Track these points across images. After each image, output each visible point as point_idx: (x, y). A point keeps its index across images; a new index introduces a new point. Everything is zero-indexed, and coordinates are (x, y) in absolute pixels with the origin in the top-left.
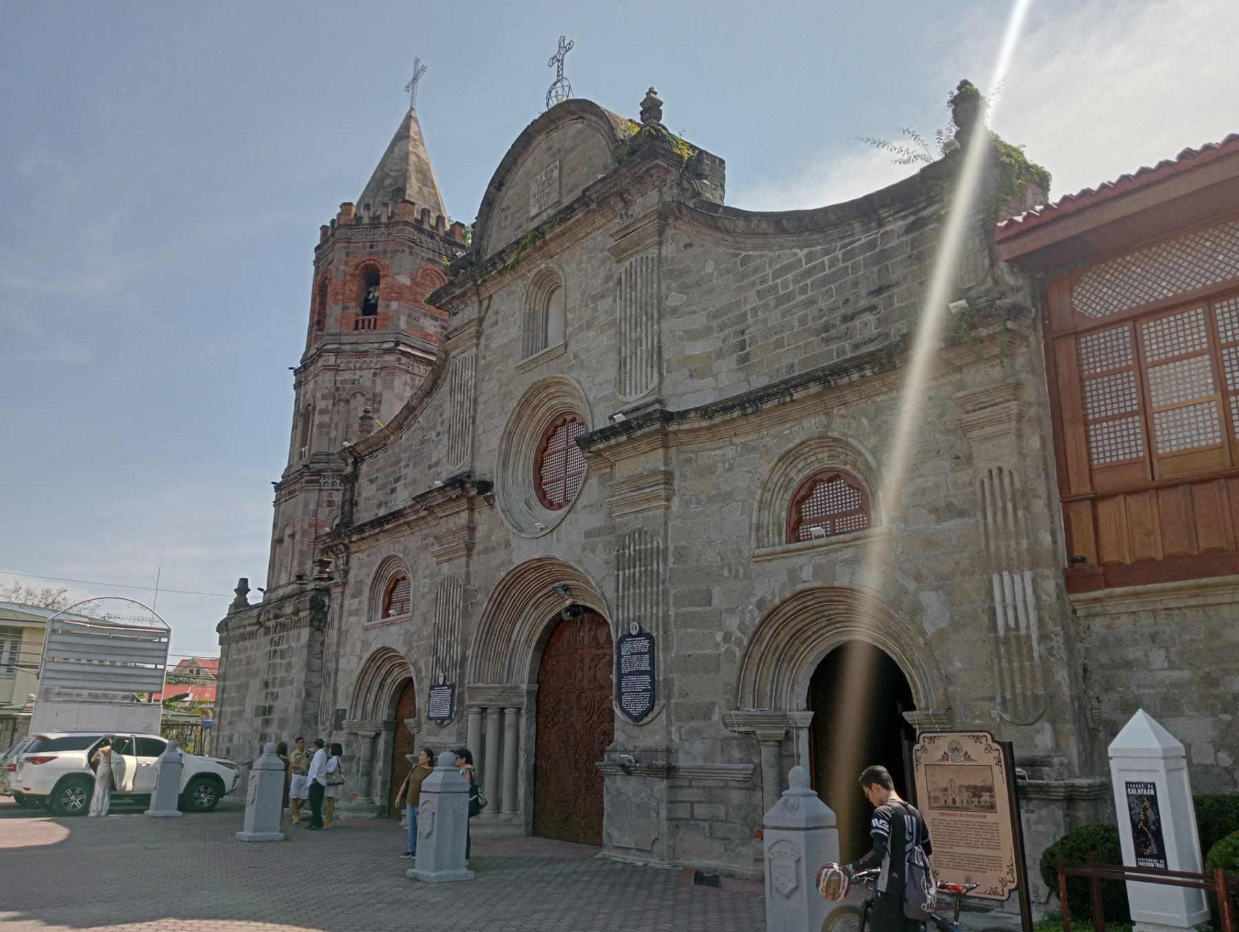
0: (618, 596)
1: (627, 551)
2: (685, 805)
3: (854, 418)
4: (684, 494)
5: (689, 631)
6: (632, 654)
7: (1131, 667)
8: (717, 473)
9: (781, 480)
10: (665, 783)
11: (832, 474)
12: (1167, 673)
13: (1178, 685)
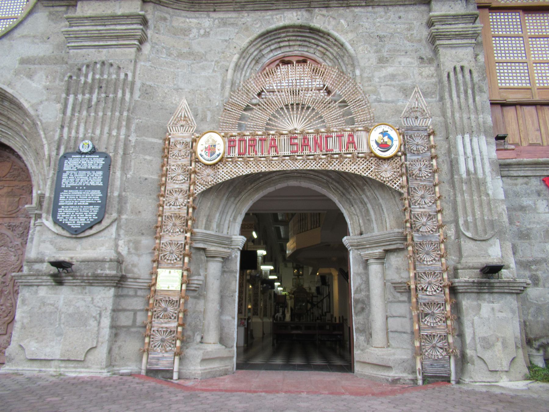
0: (63, 120)
1: (83, 79)
3: (334, 18)
4: (156, 44)
5: (148, 158)
6: (78, 170)
7: (525, 210)
8: (191, 36)
10: (112, 291)
11: (301, 59)
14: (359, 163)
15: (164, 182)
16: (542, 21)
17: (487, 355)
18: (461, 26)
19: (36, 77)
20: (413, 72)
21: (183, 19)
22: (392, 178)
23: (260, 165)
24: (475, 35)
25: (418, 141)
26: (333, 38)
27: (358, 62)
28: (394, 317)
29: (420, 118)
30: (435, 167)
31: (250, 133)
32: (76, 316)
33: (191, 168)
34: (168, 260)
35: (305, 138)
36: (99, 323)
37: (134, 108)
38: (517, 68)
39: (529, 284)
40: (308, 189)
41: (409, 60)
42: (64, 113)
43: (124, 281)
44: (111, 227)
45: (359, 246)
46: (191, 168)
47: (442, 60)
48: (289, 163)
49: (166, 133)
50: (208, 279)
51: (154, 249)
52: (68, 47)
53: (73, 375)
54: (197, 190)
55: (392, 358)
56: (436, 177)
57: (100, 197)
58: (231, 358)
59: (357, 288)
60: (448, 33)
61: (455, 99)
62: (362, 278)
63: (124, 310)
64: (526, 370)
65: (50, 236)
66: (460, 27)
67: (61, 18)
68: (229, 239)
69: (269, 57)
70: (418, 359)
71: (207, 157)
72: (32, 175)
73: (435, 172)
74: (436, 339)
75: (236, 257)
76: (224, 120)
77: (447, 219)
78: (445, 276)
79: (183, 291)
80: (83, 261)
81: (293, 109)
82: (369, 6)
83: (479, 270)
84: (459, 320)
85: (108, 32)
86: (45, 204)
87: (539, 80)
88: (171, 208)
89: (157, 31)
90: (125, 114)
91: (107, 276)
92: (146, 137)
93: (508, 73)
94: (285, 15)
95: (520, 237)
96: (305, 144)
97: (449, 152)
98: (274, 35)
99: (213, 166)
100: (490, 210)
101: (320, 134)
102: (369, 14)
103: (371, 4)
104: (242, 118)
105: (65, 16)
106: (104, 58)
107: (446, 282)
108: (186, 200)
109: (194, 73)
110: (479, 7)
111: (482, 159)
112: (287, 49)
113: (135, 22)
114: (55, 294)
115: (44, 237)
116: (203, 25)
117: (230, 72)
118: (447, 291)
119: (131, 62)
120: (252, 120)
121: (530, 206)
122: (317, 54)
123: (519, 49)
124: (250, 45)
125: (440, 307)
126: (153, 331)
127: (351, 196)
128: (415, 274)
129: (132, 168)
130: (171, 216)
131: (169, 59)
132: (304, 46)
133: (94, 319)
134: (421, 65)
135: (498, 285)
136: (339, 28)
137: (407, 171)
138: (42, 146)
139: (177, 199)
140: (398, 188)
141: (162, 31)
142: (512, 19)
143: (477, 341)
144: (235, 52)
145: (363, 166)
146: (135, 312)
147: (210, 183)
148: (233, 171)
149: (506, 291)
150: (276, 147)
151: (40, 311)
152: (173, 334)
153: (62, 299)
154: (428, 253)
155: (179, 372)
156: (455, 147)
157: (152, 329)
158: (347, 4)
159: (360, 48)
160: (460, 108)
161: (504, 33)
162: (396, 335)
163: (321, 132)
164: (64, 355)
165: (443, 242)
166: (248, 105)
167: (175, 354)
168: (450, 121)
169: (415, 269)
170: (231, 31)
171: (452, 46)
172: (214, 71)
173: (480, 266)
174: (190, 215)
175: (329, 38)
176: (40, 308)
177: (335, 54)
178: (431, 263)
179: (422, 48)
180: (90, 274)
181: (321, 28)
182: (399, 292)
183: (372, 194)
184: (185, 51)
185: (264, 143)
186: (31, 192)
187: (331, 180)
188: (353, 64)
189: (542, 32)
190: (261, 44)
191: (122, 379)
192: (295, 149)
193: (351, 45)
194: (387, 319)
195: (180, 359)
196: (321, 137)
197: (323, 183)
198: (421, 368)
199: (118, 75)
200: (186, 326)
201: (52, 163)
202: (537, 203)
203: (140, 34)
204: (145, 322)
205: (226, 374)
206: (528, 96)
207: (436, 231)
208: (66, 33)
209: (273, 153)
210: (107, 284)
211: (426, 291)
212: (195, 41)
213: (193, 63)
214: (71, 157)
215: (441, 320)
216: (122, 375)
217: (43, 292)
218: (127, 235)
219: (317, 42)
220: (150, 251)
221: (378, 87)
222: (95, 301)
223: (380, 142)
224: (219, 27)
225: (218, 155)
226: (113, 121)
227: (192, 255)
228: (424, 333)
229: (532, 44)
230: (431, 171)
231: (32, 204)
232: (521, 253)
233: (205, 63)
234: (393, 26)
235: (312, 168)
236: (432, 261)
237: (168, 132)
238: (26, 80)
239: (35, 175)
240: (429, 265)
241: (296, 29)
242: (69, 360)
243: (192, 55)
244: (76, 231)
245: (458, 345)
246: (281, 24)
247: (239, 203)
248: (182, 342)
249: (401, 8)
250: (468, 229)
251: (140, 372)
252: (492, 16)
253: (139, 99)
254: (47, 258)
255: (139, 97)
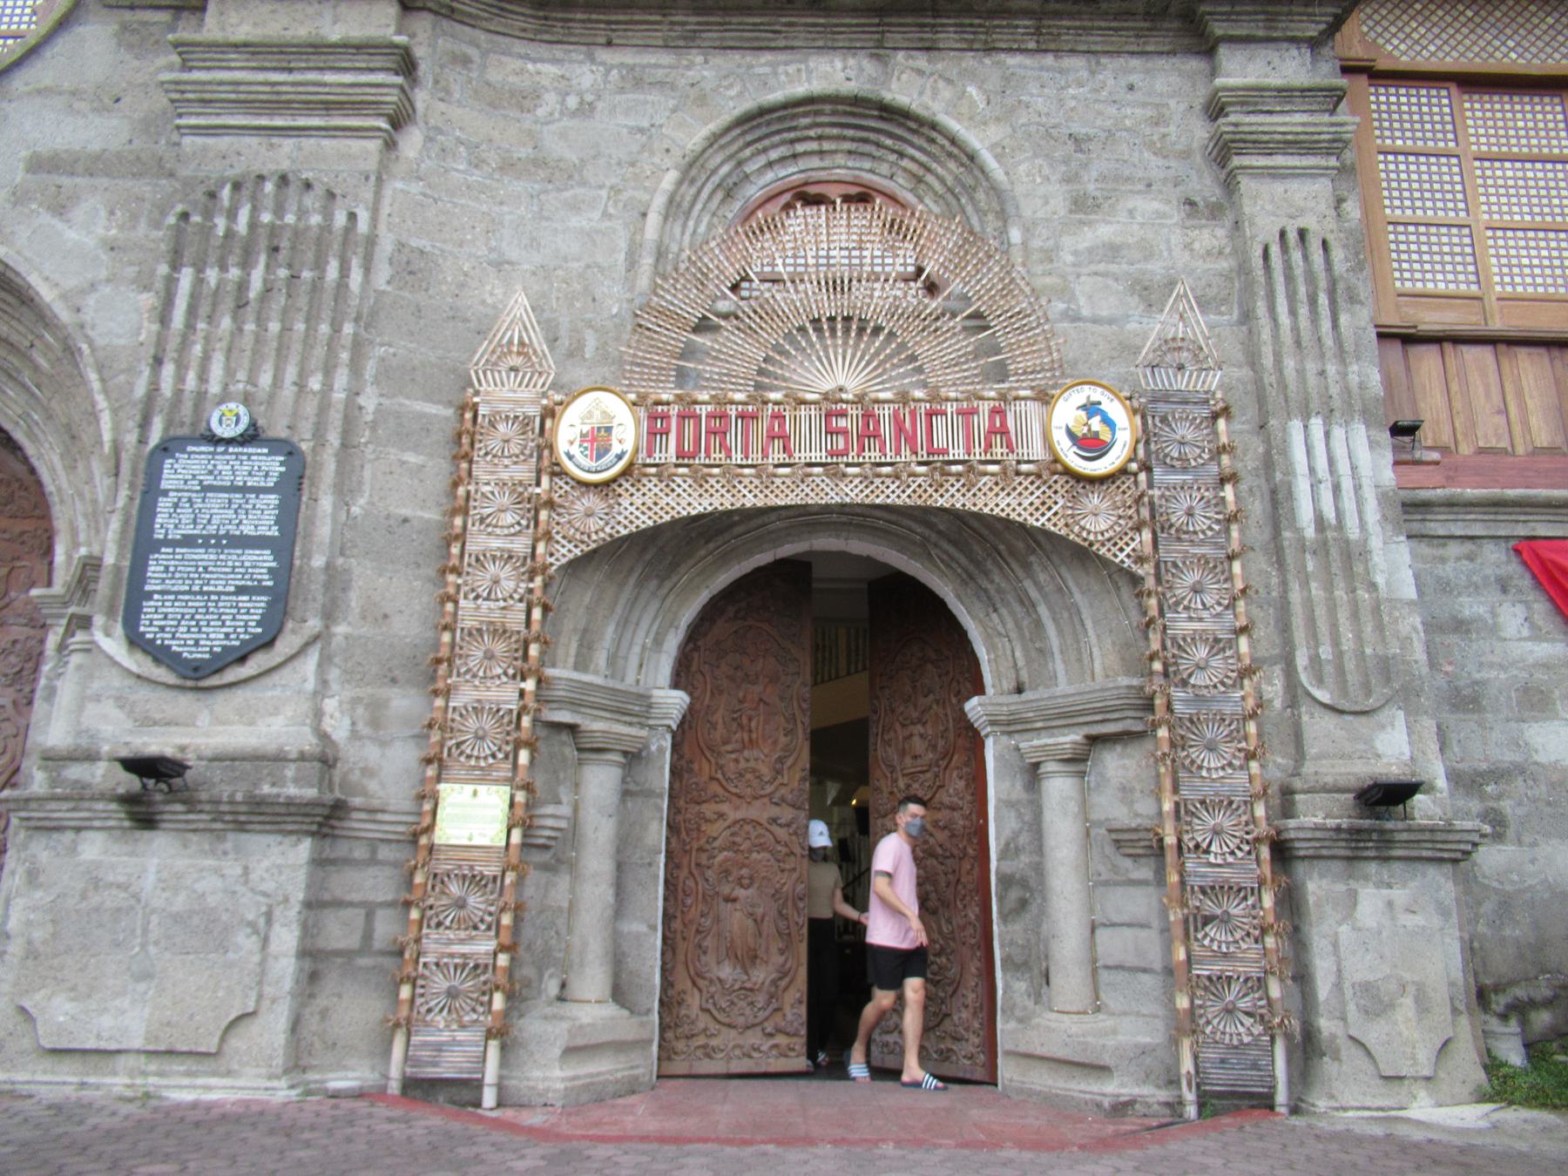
0: (160, 342)
1: (221, 223)
2: (350, 912)
3: (949, 81)
4: (439, 131)
5: (412, 458)
6: (206, 489)
7: (1468, 631)
8: (540, 112)
9: (725, 169)
10: (305, 848)
11: (854, 190)
12: (1529, 645)
13: (1546, 666)
14: (1020, 489)
15: (458, 530)
16: (1509, 115)
17: (1373, 1034)
18: (1299, 118)
19: (79, 213)
20: (1168, 241)
21: (518, 64)
22: (1111, 533)
23: (740, 487)
24: (1336, 146)
25: (1185, 431)
26: (945, 137)
27: (1017, 207)
28: (1113, 925)
29: (1189, 367)
30: (1231, 507)
31: (713, 397)
32: (196, 920)
33: (538, 490)
34: (469, 757)
35: (868, 415)
36: (265, 941)
37: (374, 313)
38: (1445, 240)
39: (1483, 836)
40: (869, 560)
41: (1156, 205)
42: (164, 319)
43: (340, 819)
44: (301, 659)
45: (1012, 725)
46: (538, 490)
47: (1247, 210)
48: (823, 485)
49: (464, 389)
50: (582, 813)
51: (430, 726)
52: (178, 127)
53: (188, 1096)
54: (557, 555)
55: (1111, 1042)
56: (1235, 534)
57: (270, 570)
58: (644, 1044)
59: (1007, 844)
60: (1265, 138)
61: (1284, 319)
62: (1020, 816)
63: (339, 904)
64: (1481, 1076)
65: (117, 681)
66: (1295, 121)
67: (157, 42)
68: (644, 699)
69: (762, 182)
70: (1186, 1043)
71: (586, 463)
72: (55, 499)
73: (1231, 519)
74: (1235, 987)
75: (661, 750)
76: (635, 356)
77: (1262, 652)
78: (1260, 811)
79: (512, 850)
80: (216, 758)
81: (833, 331)
82: (1046, 51)
83: (1351, 796)
84: (1297, 938)
85: (300, 89)
86: (103, 587)
87: (1501, 275)
88: (478, 607)
89: (442, 95)
90: (348, 329)
91: (290, 803)
92: (408, 398)
93: (1419, 252)
94: (812, 64)
95: (1454, 705)
96: (869, 433)
97: (1268, 464)
98: (780, 119)
99: (604, 488)
100: (1380, 628)
101: (912, 405)
102: (1045, 74)
103: (1052, 46)
104: (688, 352)
105: (170, 37)
106: (285, 165)
107: (1263, 829)
108: (523, 585)
109: (548, 219)
110: (1346, 70)
111: (1358, 488)
112: (815, 162)
113: (378, 65)
114: (132, 854)
115: (96, 685)
116: (574, 82)
117: (654, 219)
118: (1265, 852)
119: (367, 178)
120: (716, 358)
121: (1480, 619)
122: (901, 181)
123: (1447, 187)
124: (711, 145)
125: (1245, 898)
126: (425, 965)
127: (992, 582)
128: (1177, 804)
129: (367, 488)
130: (479, 630)
131: (476, 177)
132: (862, 154)
133: (249, 930)
134: (1189, 223)
135: (1404, 836)
136: (964, 110)
137: (1153, 517)
138: (94, 416)
139: (496, 582)
140: (1128, 562)
141: (457, 96)
142: (1429, 105)
143: (1349, 993)
144: (668, 162)
145: (1032, 498)
146: (370, 909)
147: (594, 537)
148: (662, 503)
149: (1425, 853)
150: (785, 438)
151: (83, 905)
152: (484, 973)
153: (152, 869)
154: (1211, 748)
155: (500, 1087)
156: (1285, 452)
157: (422, 960)
158: (986, 42)
159: (1022, 168)
160: (1298, 343)
161: (1409, 143)
162: (1120, 976)
163: (914, 400)
164: (157, 1038)
165: (1253, 715)
166: (705, 318)
167: (489, 1034)
168: (1269, 378)
169: (1176, 790)
170: (656, 107)
171: (1275, 174)
172: (606, 215)
173: (1353, 783)
174: (535, 627)
175: (934, 135)
176: (84, 897)
177: (950, 180)
178: (1221, 773)
179: (1193, 173)
180: (239, 797)
181: (913, 107)
182: (1130, 856)
183: (1052, 577)
184: (523, 155)
185: (752, 425)
186: (49, 551)
187: (934, 537)
188: (1003, 210)
189: (1508, 145)
190: (741, 142)
191: (335, 1107)
192: (841, 446)
193: (998, 157)
194: (1093, 931)
195: (503, 1048)
196: (913, 413)
197: (914, 543)
198: (1192, 1071)
199: (328, 215)
200: (521, 951)
201: (126, 468)
202: (1499, 610)
203: (395, 99)
204: (401, 939)
205: (633, 1092)
206: (1474, 319)
207: (1234, 686)
208: (173, 87)
209: (777, 455)
210: (290, 827)
211: (1207, 851)
212: (553, 127)
213: (546, 192)
214: (183, 451)
215: (1248, 934)
216: (335, 1095)
217: (93, 847)
218: (348, 681)
219: (898, 146)
220: (416, 731)
221: (1071, 278)
222: (254, 876)
223: (1081, 431)
224: (622, 90)
225: (619, 457)
226: (312, 347)
227: (539, 744)
228: (1201, 971)
229: (1484, 177)
230: (1220, 517)
231: (49, 584)
232: (1456, 749)
233: (580, 191)
234: (1112, 110)
235: (889, 501)
236: (1223, 768)
237: (472, 385)
238: (46, 218)
239: (62, 501)
240: (1214, 780)
241: (840, 108)
242: (171, 1053)
243: (540, 165)
244: (196, 669)
245: (1295, 1003)
246: (800, 90)
247: (672, 597)
248: (510, 997)
249: (1135, 62)
250: (1320, 681)
251: (385, 1087)
252: (1377, 95)
253: (389, 289)
254: (106, 748)
255: (389, 283)
